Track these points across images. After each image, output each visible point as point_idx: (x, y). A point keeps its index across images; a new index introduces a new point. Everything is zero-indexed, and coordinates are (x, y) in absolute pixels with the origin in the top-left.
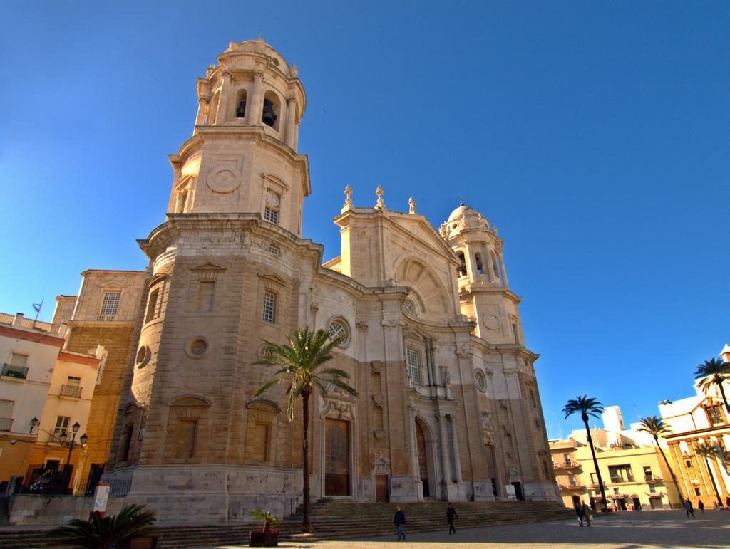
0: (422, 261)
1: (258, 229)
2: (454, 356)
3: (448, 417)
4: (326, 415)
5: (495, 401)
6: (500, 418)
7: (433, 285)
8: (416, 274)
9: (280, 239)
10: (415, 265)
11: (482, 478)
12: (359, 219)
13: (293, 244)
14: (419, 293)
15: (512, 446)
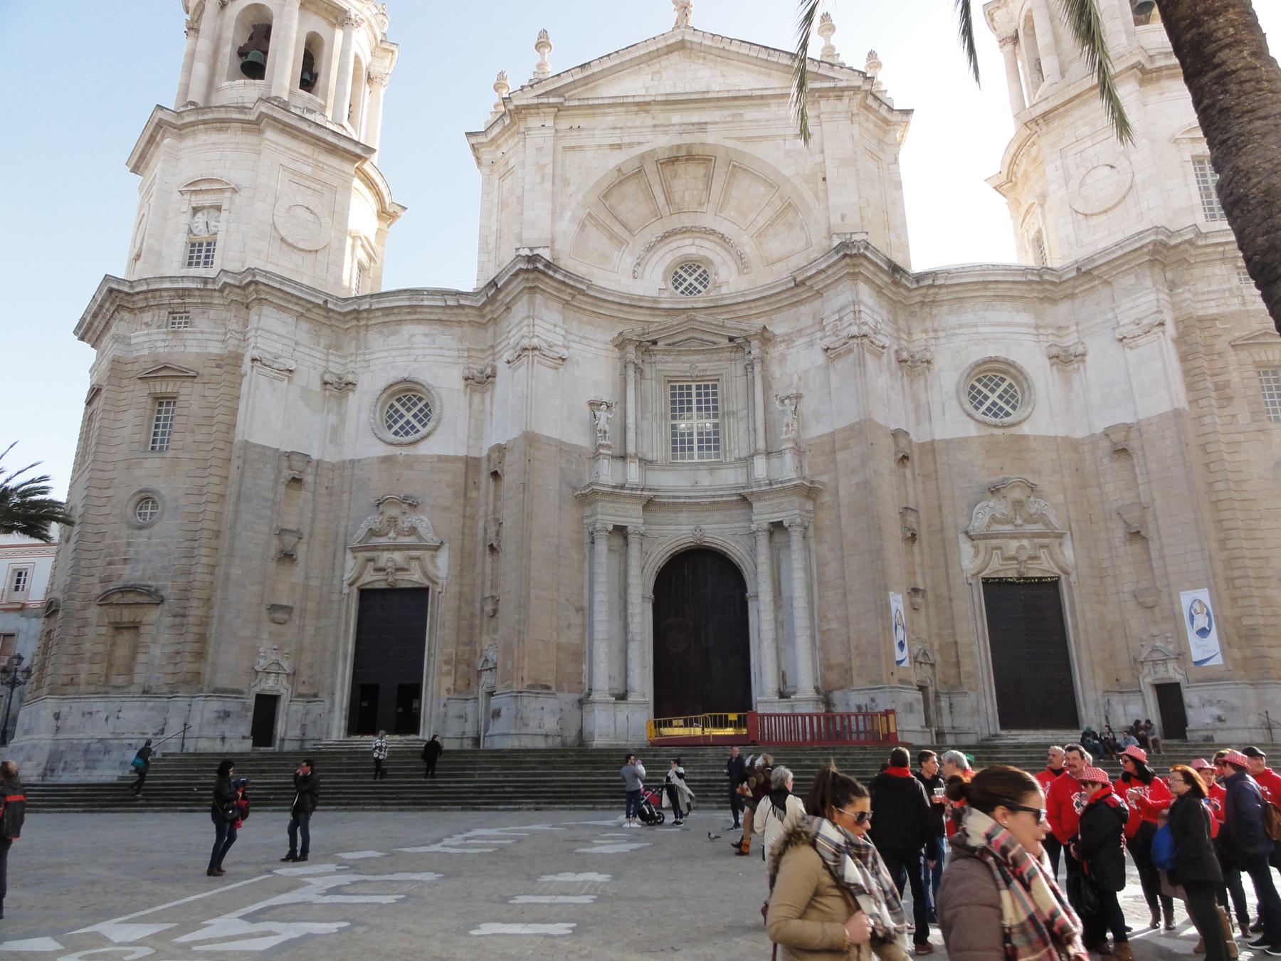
0: (690, 146)
1: (136, 298)
2: (820, 359)
3: (777, 527)
4: (358, 584)
5: (1093, 440)
6: (1109, 488)
7: (762, 190)
8: (700, 185)
9: (179, 297)
10: (681, 168)
11: (872, 682)
12: (493, 140)
13: (209, 293)
14: (724, 228)
15: (1152, 569)
